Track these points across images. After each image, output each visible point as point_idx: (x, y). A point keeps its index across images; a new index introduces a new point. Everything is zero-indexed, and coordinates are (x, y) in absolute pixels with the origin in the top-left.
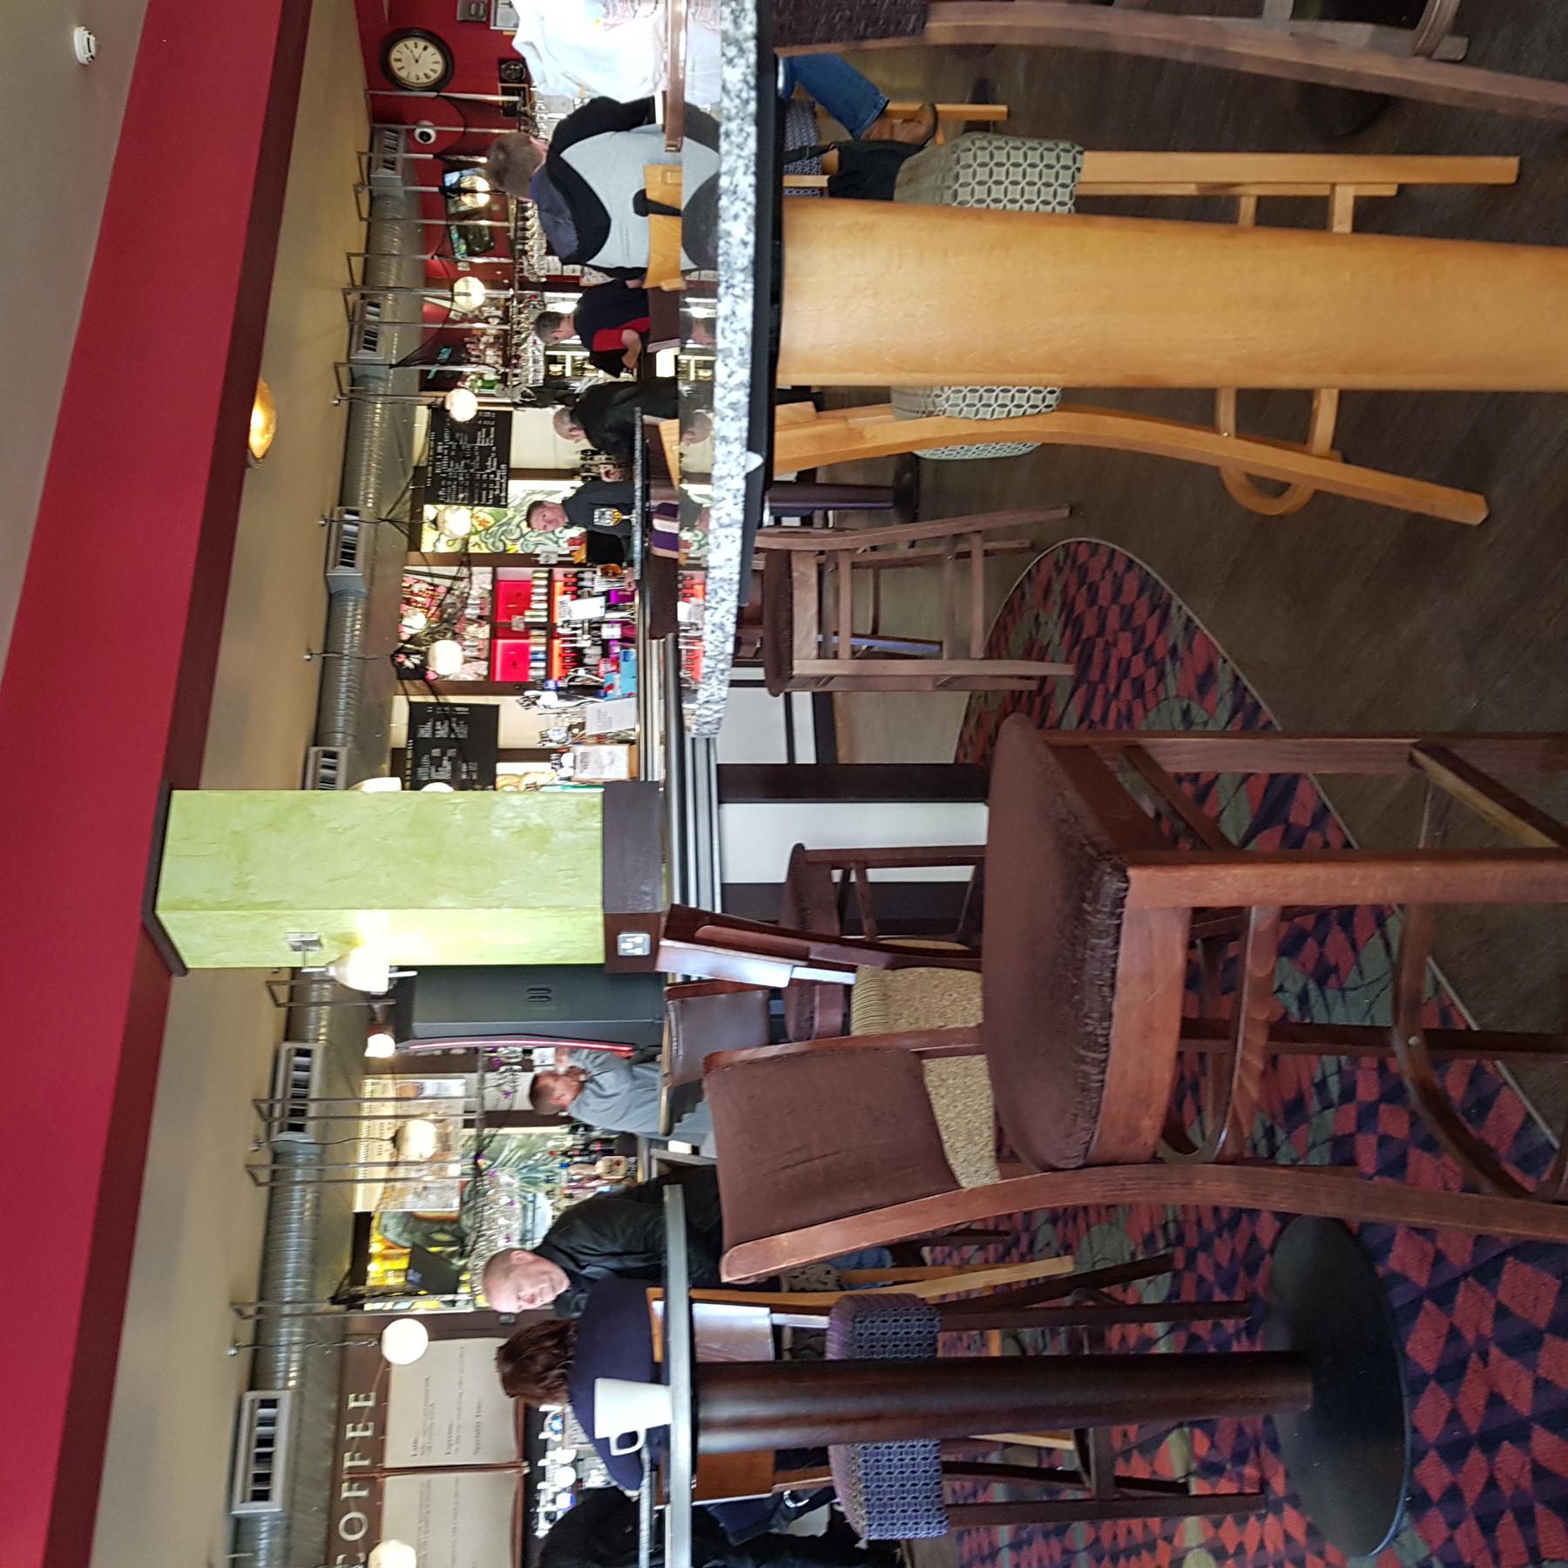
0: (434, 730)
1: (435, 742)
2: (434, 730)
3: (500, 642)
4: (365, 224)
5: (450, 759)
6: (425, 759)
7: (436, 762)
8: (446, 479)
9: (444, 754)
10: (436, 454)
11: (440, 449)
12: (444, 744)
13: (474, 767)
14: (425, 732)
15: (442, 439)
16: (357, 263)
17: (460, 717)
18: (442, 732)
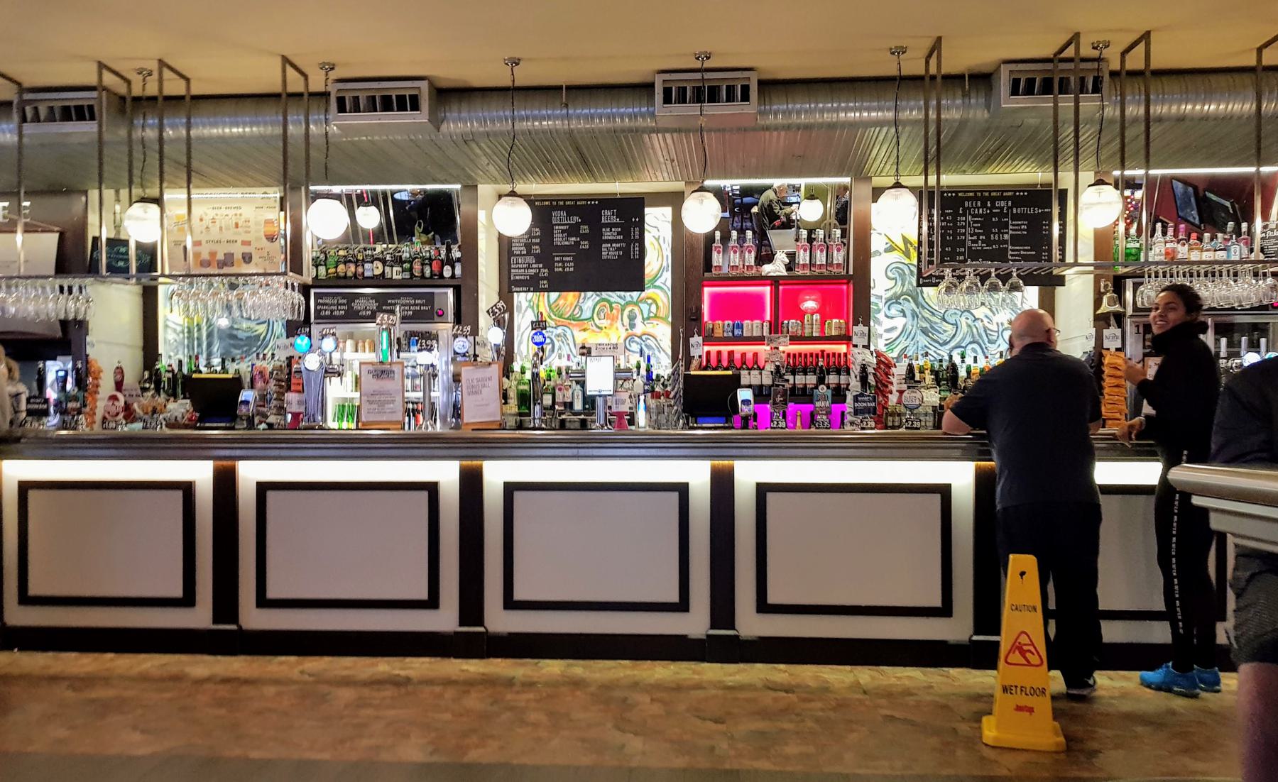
0: (611, 226)
1: (597, 226)
2: (611, 226)
3: (768, 289)
4: (1251, 61)
5: (578, 244)
6: (575, 219)
7: (572, 231)
8: (956, 214)
9: (584, 237)
10: (993, 200)
11: (1003, 203)
12: (596, 239)
13: (570, 268)
14: (608, 216)
15: (1015, 205)
16: (1135, 61)
17: (627, 251)
18: (607, 234)
